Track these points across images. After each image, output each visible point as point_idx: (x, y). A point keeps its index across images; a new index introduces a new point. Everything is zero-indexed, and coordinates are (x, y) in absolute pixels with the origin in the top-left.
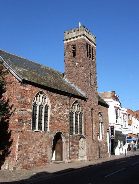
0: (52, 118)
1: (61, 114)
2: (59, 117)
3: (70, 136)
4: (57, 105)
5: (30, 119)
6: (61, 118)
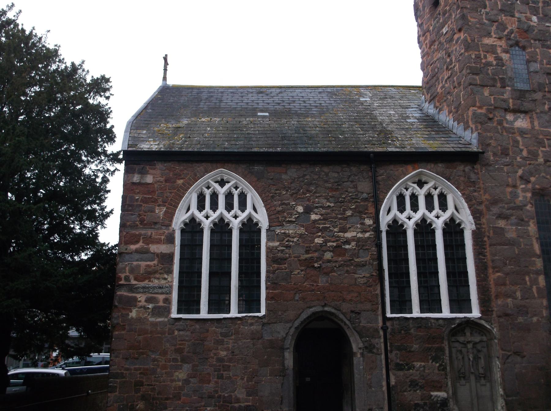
1: (326, 242)
2: (316, 255)
3: (384, 323)
4: (300, 209)
5: (165, 279)
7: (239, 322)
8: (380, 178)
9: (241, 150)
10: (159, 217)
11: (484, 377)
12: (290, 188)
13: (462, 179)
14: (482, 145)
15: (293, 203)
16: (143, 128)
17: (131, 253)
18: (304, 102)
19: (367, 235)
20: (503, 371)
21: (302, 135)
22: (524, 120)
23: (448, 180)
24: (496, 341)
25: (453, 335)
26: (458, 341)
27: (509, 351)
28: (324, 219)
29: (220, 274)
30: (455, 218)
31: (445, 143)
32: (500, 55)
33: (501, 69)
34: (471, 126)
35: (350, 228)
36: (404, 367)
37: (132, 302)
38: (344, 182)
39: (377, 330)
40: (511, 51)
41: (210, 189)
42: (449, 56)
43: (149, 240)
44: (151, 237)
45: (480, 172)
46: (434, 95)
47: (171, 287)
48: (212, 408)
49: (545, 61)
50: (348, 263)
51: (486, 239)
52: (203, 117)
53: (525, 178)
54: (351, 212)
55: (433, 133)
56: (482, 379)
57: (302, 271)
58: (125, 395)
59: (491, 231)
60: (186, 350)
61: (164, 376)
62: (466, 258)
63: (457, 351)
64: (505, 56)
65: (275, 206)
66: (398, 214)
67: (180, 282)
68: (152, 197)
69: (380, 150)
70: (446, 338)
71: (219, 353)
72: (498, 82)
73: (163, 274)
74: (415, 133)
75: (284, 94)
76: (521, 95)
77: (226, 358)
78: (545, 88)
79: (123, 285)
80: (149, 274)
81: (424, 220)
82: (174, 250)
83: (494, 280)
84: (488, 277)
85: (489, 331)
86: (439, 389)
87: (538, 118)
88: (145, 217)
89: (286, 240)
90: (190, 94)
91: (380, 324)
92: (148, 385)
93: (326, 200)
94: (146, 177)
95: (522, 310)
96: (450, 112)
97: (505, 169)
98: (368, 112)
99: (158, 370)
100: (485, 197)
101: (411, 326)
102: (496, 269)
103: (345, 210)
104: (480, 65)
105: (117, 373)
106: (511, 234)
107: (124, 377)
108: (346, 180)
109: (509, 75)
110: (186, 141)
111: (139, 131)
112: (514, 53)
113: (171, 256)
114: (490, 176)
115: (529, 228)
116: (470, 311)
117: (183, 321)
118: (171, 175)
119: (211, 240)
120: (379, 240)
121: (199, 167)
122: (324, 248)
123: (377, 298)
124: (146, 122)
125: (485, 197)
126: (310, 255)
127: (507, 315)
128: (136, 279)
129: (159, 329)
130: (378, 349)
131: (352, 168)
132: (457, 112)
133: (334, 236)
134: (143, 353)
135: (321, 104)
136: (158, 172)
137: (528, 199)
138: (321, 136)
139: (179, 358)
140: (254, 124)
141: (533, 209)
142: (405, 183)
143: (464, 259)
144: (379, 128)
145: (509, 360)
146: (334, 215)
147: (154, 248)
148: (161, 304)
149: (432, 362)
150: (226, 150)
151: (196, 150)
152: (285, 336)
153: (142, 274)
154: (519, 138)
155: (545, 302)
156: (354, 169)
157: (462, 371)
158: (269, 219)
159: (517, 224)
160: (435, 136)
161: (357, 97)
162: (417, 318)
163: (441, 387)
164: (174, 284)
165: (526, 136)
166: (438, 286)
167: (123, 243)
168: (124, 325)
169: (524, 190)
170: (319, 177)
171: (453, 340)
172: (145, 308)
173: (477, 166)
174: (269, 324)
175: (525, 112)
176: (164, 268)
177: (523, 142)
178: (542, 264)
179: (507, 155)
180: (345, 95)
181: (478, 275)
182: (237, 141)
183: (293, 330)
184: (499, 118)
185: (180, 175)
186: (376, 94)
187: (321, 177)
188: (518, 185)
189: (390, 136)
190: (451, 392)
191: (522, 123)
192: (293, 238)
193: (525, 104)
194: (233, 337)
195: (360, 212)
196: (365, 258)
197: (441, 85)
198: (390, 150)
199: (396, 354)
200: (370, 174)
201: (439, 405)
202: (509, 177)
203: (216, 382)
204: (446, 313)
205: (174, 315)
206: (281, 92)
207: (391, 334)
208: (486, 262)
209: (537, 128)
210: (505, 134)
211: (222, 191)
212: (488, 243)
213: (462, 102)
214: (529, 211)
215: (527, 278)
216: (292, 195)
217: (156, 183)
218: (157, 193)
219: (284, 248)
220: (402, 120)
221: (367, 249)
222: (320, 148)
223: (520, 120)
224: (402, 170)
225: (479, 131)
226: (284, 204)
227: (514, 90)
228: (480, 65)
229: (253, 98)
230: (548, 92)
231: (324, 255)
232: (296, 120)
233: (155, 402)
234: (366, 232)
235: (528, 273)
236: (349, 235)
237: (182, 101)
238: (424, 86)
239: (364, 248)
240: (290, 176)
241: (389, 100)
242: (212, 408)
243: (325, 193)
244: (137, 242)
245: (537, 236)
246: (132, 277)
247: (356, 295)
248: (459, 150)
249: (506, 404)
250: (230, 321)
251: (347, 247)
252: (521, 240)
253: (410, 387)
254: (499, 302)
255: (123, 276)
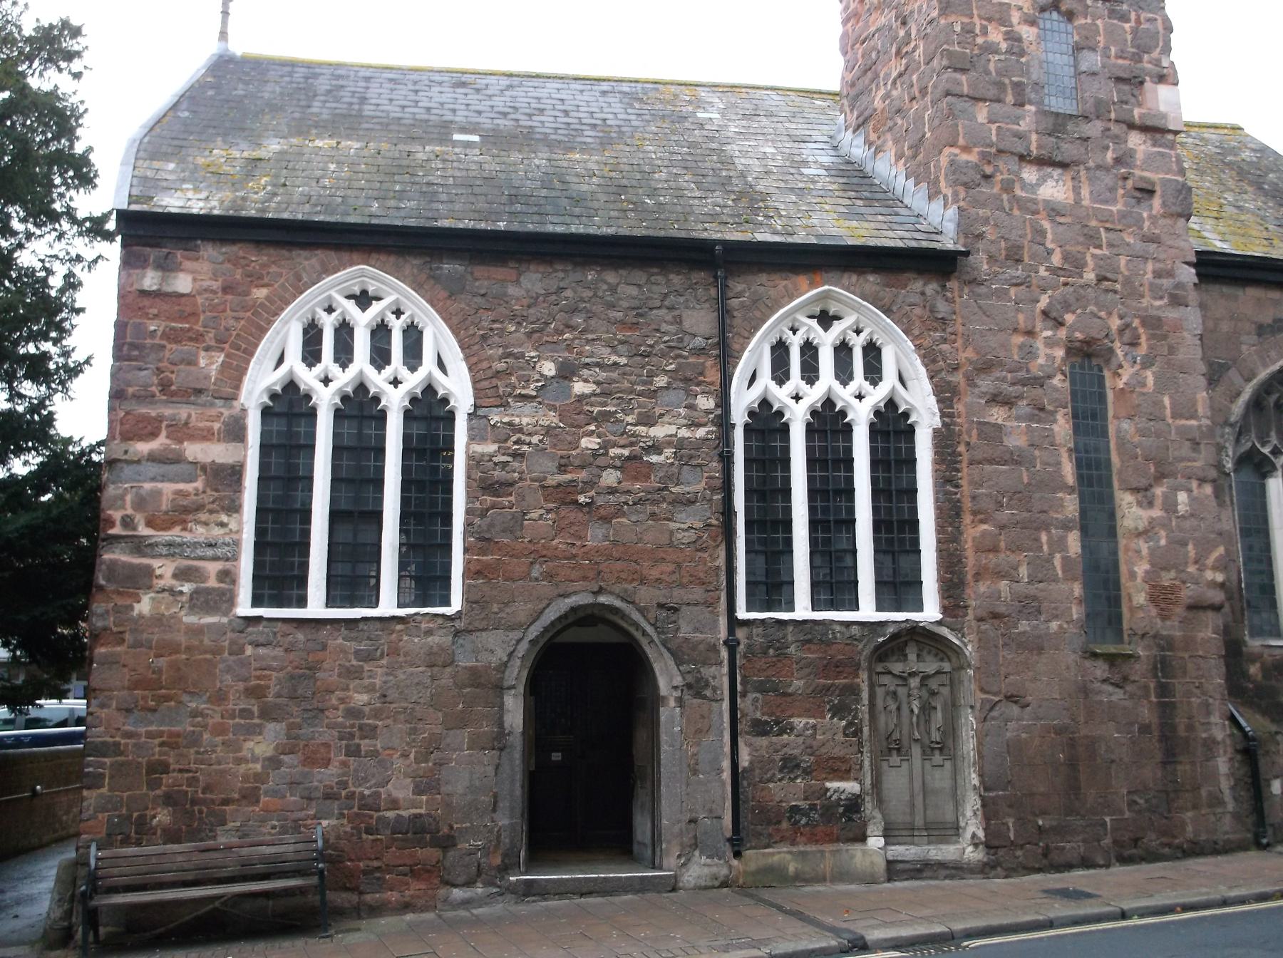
0: (486, 484)
1: (606, 446)
2: (582, 475)
3: (731, 631)
4: (549, 368)
5: (223, 525)
6: (610, 478)
7: (399, 627)
8: (734, 303)
9: (412, 222)
10: (207, 377)
11: (941, 749)
12: (525, 318)
13: (918, 311)
14: (966, 237)
15: (533, 354)
16: (166, 157)
17: (138, 462)
18: (566, 113)
19: (701, 432)
20: (981, 738)
21: (558, 194)
22: (1061, 183)
23: (887, 311)
24: (971, 672)
25: (882, 658)
26: (890, 673)
27: (995, 694)
28: (603, 394)
29: (356, 515)
30: (897, 400)
31: (885, 227)
32: (1017, 28)
33: (1018, 61)
34: (944, 190)
35: (662, 415)
36: (772, 728)
37: (140, 579)
38: (651, 309)
39: (713, 648)
40: (1041, 23)
41: (334, 315)
42: (904, 23)
43: (182, 431)
44: (186, 424)
45: (957, 299)
46: (866, 114)
47: (237, 543)
48: (334, 822)
49: (1113, 49)
50: (656, 496)
51: (961, 448)
52: (319, 136)
53: (1054, 314)
54: (666, 379)
55: (860, 203)
56: (937, 752)
57: (549, 511)
58: (125, 794)
59: (975, 432)
60: (273, 690)
61: (219, 749)
62: (916, 491)
63: (887, 693)
64: (1028, 33)
65: (490, 358)
66: (773, 386)
67: (260, 532)
68: (189, 330)
69: (734, 235)
70: (864, 664)
71: (351, 698)
72: (1010, 91)
73: (217, 512)
74: (819, 200)
75: (518, 92)
76: (1057, 124)
77: (367, 709)
78: (1109, 112)
79: (117, 538)
80: (182, 513)
81: (829, 402)
82: (245, 456)
83: (974, 539)
84: (961, 534)
85: (957, 651)
86: (844, 775)
87: (1089, 179)
88: (173, 376)
89: (514, 439)
90: (287, 79)
91: (723, 634)
92: (181, 771)
93: (609, 350)
94: (175, 278)
95: (1030, 606)
96: (899, 157)
97: (1013, 291)
98: (714, 146)
99: (205, 736)
100: (965, 355)
101: (790, 638)
102: (981, 515)
103: (651, 375)
104: (972, 50)
105: (104, 743)
106: (1016, 440)
107: (121, 754)
108: (658, 304)
109: (1034, 77)
110: (275, 194)
111: (156, 164)
112: (1048, 26)
113: (234, 474)
114: (980, 307)
115: (1056, 428)
116: (920, 608)
117: (264, 623)
118: (238, 277)
119: (336, 435)
120: (728, 446)
121: (308, 260)
122: (601, 461)
123: (717, 575)
124: (176, 142)
125: (965, 355)
126: (568, 477)
127: (996, 616)
128: (149, 524)
129: (206, 641)
130: (715, 689)
131: (671, 276)
132: (915, 156)
133: (624, 433)
134: (168, 698)
135: (605, 120)
136: (204, 267)
137: (1058, 361)
138: (603, 198)
139: (255, 709)
140: (444, 161)
141: (1067, 384)
142: (791, 314)
143: (912, 492)
144: (737, 185)
145: (994, 714)
146: (627, 385)
147: (195, 451)
148: (212, 583)
149: (832, 718)
150: (374, 221)
151: (300, 217)
152: (505, 659)
153: (166, 513)
154: (1046, 225)
155: (1077, 589)
156: (676, 279)
157: (896, 736)
158: (475, 389)
159: (1031, 418)
160: (863, 210)
161: (690, 109)
162: (805, 622)
163: (848, 771)
164: (244, 536)
165: (1062, 220)
166: (854, 552)
167: (117, 436)
168: (121, 633)
169: (1050, 343)
170: (595, 295)
171: (879, 670)
172: (171, 591)
173: (953, 284)
174: (470, 632)
175: (1064, 165)
176: (221, 499)
177: (1055, 234)
178: (1077, 507)
179: (1019, 261)
180: (662, 103)
181: (940, 529)
182: (400, 200)
183: (524, 646)
184: (1006, 176)
185: (261, 277)
186: (735, 106)
187: (600, 294)
188: (1038, 329)
189: (761, 204)
190: (868, 781)
191: (1054, 189)
192: (530, 434)
193: (1065, 146)
194: (384, 662)
195: (687, 380)
196: (694, 484)
197: (882, 92)
198: (760, 237)
199: (756, 700)
200: (713, 292)
201: (841, 810)
202: (1018, 310)
203: (344, 764)
204: (867, 610)
205: (244, 607)
206: (510, 87)
207: (745, 656)
208: (959, 501)
209: (1086, 203)
210: (1016, 212)
211: (362, 321)
212: (965, 458)
213: (928, 135)
214: (1056, 389)
215: (1044, 538)
216: (529, 335)
217: (199, 293)
218: (202, 317)
219: (509, 459)
220: (792, 171)
221: (699, 465)
222: (599, 226)
223: (1050, 183)
224: (785, 287)
225: (962, 204)
226: (510, 355)
227: (1043, 113)
228: (972, 50)
229: (444, 98)
230: (1116, 121)
231: (600, 476)
232: (545, 156)
233: (196, 808)
234: (699, 425)
235: (1046, 526)
236: (659, 432)
237: (266, 95)
238: (845, 93)
239: (694, 462)
240: (528, 291)
241: (764, 119)
242: (334, 822)
243: (607, 332)
244: (154, 435)
245: (1072, 445)
246: (140, 519)
247: (671, 567)
248: (914, 244)
249: (983, 806)
250: (378, 625)
251: (654, 459)
252: (1037, 453)
253: (781, 771)
254: (983, 588)
255: (117, 515)
